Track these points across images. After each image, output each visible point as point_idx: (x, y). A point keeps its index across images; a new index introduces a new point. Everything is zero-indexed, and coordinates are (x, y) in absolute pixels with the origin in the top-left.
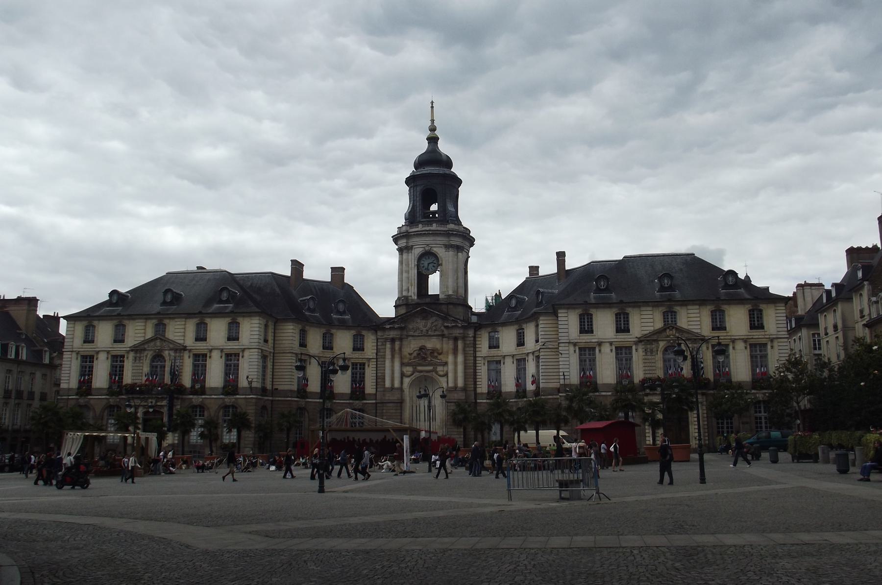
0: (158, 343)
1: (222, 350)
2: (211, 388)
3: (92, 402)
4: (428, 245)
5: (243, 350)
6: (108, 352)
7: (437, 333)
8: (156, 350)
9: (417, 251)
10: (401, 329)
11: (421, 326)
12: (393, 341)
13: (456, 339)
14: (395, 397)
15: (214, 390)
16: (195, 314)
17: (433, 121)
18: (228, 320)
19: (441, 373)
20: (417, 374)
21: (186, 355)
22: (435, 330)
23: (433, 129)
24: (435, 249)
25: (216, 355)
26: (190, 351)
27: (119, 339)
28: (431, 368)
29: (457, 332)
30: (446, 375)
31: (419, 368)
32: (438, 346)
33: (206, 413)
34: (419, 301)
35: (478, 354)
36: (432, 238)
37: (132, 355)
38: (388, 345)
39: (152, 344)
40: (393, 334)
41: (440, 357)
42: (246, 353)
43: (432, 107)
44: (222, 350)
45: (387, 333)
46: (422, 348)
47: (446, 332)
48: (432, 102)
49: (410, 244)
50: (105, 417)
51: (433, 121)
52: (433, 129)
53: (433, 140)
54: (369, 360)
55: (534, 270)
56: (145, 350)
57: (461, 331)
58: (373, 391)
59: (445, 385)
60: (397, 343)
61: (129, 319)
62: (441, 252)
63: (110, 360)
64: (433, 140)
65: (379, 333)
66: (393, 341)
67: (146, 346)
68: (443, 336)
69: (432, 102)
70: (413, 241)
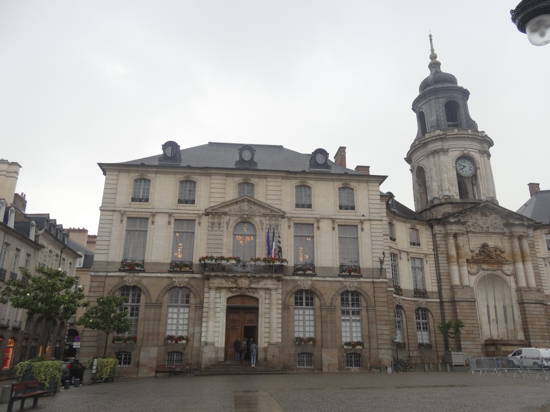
0: (245, 206)
1: (333, 221)
2: (323, 268)
3: (145, 282)
4: (466, 148)
5: (362, 222)
6: (170, 215)
7: (497, 231)
8: (245, 212)
9: (454, 154)
10: (464, 223)
11: (481, 224)
12: (455, 236)
13: (520, 238)
14: (468, 296)
15: (327, 270)
16: (296, 173)
17: (432, 50)
18: (339, 184)
19: (508, 272)
20: (481, 272)
21: (284, 224)
22: (496, 228)
23: (433, 57)
24: (472, 153)
25: (325, 225)
26: (289, 219)
27: (187, 200)
28: (496, 267)
29: (519, 231)
30: (515, 275)
31: (485, 266)
32: (500, 245)
33: (317, 301)
34: (460, 201)
35: (538, 255)
36: (469, 143)
37: (205, 220)
38: (451, 240)
39: (236, 207)
40: (454, 228)
41: (503, 255)
42: (366, 226)
43: (431, 40)
44: (333, 221)
45: (449, 227)
46: (484, 246)
47: (506, 230)
48: (430, 36)
49: (445, 147)
50: (165, 305)
51: (432, 50)
52: (433, 57)
53: (435, 65)
54: (426, 255)
55: (534, 188)
56: (225, 214)
57: (525, 230)
58: (436, 289)
59: (513, 285)
60: (461, 239)
61: (202, 174)
62: (476, 156)
63: (172, 225)
64: (435, 65)
65: (438, 228)
66: (455, 236)
67: (226, 209)
68: (503, 234)
69: (430, 36)
70: (446, 145)
